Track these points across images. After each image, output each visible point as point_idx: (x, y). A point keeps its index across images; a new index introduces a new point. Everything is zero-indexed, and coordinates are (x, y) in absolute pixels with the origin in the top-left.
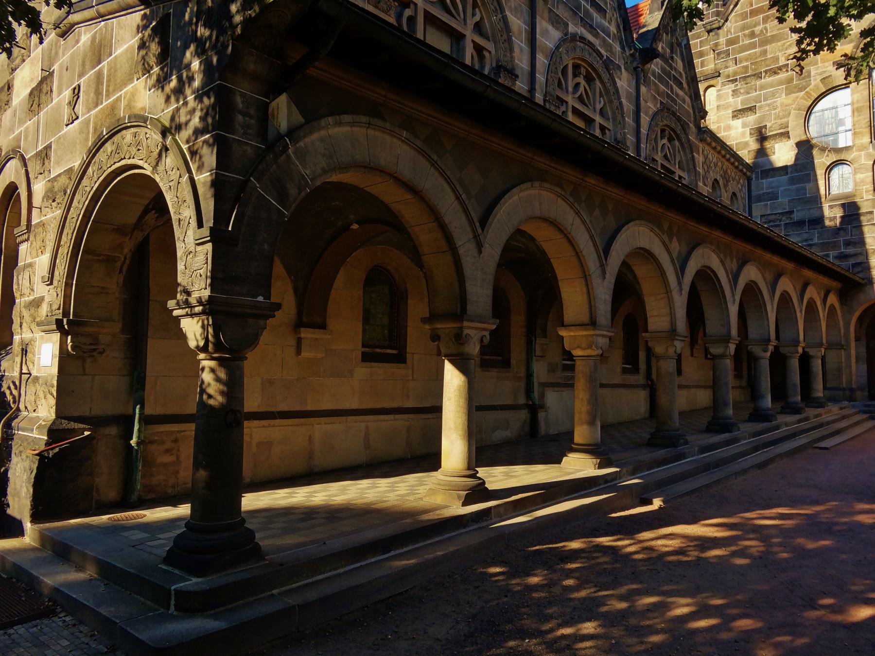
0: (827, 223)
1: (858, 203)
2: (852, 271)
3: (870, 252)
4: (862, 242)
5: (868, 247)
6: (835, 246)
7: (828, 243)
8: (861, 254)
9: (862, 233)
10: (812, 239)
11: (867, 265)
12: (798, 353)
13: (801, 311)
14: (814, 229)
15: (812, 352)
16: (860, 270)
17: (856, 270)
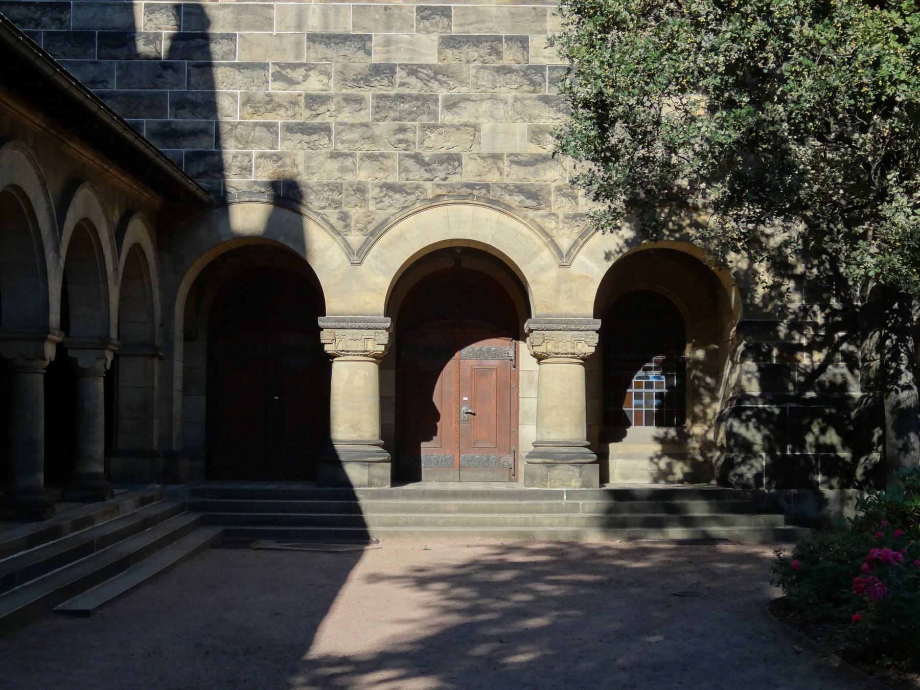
0: (142, 47)
1: (207, 10)
2: (187, 170)
3: (225, 128)
4: (210, 106)
5: (223, 119)
6: (154, 106)
7: (139, 96)
8: (205, 132)
9: (210, 84)
10: (104, 82)
11: (216, 159)
12: (44, 358)
13: (57, 249)
14: (113, 57)
15: (83, 359)
16: (201, 170)
17: (194, 169)
